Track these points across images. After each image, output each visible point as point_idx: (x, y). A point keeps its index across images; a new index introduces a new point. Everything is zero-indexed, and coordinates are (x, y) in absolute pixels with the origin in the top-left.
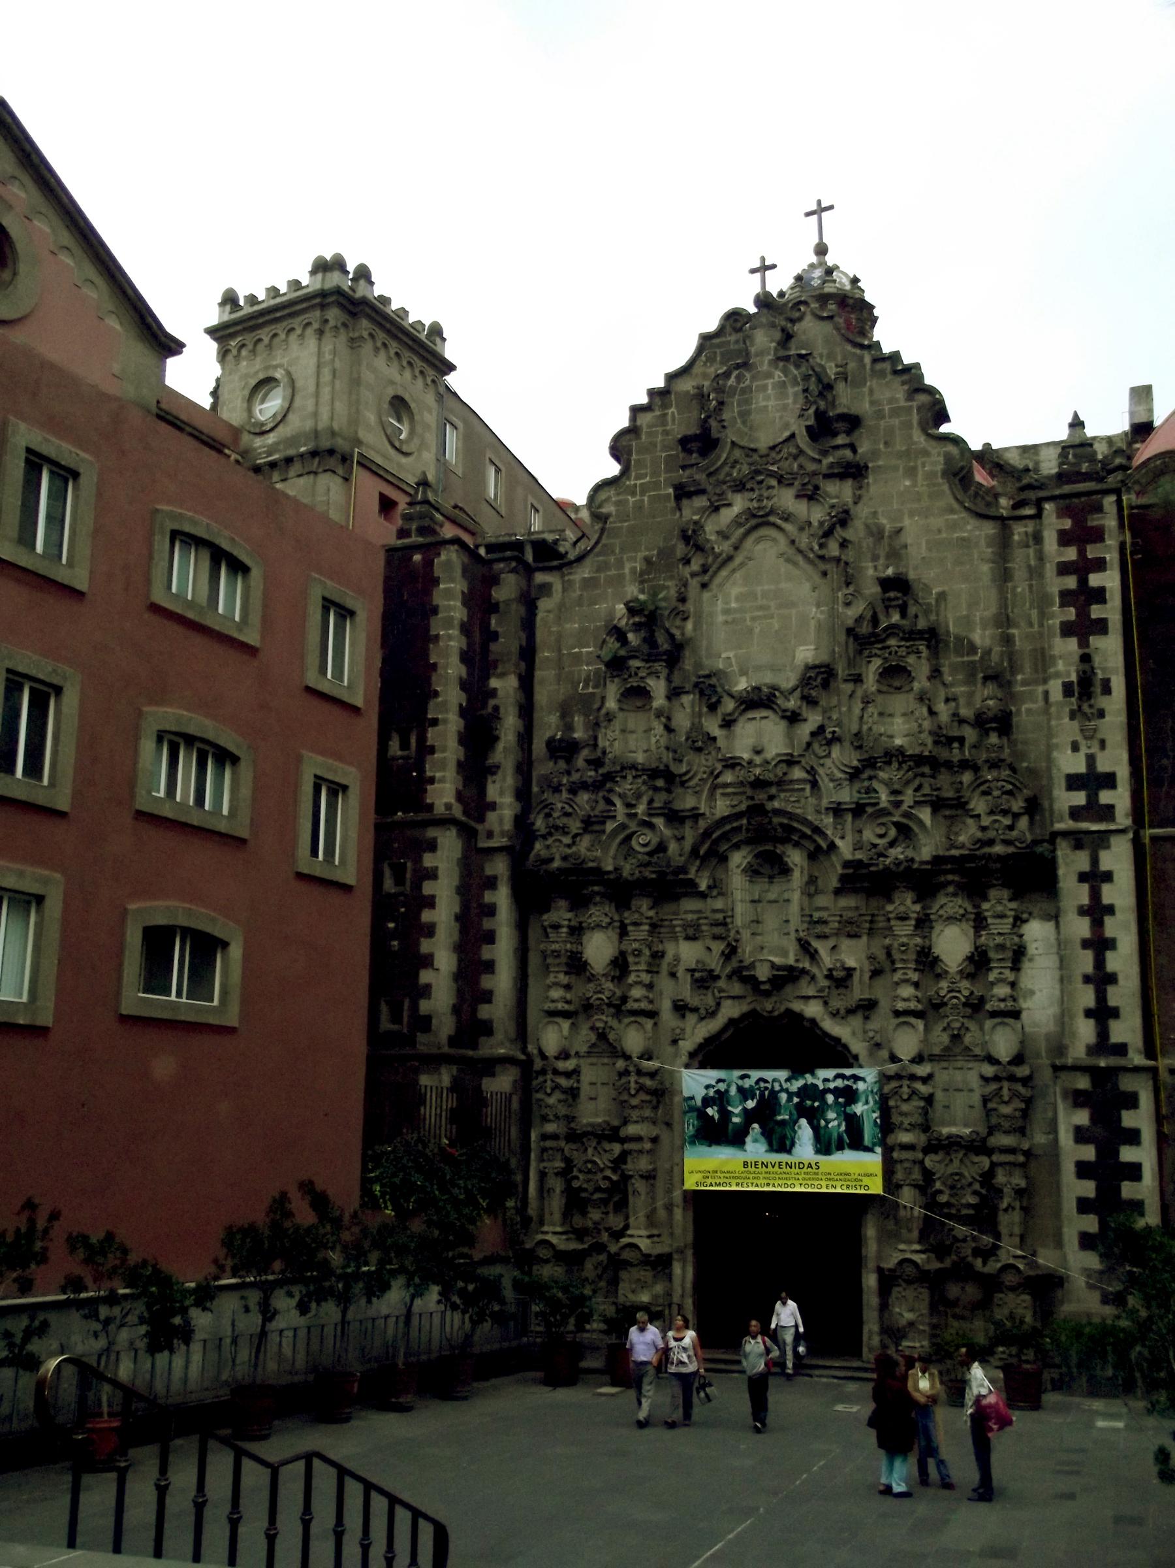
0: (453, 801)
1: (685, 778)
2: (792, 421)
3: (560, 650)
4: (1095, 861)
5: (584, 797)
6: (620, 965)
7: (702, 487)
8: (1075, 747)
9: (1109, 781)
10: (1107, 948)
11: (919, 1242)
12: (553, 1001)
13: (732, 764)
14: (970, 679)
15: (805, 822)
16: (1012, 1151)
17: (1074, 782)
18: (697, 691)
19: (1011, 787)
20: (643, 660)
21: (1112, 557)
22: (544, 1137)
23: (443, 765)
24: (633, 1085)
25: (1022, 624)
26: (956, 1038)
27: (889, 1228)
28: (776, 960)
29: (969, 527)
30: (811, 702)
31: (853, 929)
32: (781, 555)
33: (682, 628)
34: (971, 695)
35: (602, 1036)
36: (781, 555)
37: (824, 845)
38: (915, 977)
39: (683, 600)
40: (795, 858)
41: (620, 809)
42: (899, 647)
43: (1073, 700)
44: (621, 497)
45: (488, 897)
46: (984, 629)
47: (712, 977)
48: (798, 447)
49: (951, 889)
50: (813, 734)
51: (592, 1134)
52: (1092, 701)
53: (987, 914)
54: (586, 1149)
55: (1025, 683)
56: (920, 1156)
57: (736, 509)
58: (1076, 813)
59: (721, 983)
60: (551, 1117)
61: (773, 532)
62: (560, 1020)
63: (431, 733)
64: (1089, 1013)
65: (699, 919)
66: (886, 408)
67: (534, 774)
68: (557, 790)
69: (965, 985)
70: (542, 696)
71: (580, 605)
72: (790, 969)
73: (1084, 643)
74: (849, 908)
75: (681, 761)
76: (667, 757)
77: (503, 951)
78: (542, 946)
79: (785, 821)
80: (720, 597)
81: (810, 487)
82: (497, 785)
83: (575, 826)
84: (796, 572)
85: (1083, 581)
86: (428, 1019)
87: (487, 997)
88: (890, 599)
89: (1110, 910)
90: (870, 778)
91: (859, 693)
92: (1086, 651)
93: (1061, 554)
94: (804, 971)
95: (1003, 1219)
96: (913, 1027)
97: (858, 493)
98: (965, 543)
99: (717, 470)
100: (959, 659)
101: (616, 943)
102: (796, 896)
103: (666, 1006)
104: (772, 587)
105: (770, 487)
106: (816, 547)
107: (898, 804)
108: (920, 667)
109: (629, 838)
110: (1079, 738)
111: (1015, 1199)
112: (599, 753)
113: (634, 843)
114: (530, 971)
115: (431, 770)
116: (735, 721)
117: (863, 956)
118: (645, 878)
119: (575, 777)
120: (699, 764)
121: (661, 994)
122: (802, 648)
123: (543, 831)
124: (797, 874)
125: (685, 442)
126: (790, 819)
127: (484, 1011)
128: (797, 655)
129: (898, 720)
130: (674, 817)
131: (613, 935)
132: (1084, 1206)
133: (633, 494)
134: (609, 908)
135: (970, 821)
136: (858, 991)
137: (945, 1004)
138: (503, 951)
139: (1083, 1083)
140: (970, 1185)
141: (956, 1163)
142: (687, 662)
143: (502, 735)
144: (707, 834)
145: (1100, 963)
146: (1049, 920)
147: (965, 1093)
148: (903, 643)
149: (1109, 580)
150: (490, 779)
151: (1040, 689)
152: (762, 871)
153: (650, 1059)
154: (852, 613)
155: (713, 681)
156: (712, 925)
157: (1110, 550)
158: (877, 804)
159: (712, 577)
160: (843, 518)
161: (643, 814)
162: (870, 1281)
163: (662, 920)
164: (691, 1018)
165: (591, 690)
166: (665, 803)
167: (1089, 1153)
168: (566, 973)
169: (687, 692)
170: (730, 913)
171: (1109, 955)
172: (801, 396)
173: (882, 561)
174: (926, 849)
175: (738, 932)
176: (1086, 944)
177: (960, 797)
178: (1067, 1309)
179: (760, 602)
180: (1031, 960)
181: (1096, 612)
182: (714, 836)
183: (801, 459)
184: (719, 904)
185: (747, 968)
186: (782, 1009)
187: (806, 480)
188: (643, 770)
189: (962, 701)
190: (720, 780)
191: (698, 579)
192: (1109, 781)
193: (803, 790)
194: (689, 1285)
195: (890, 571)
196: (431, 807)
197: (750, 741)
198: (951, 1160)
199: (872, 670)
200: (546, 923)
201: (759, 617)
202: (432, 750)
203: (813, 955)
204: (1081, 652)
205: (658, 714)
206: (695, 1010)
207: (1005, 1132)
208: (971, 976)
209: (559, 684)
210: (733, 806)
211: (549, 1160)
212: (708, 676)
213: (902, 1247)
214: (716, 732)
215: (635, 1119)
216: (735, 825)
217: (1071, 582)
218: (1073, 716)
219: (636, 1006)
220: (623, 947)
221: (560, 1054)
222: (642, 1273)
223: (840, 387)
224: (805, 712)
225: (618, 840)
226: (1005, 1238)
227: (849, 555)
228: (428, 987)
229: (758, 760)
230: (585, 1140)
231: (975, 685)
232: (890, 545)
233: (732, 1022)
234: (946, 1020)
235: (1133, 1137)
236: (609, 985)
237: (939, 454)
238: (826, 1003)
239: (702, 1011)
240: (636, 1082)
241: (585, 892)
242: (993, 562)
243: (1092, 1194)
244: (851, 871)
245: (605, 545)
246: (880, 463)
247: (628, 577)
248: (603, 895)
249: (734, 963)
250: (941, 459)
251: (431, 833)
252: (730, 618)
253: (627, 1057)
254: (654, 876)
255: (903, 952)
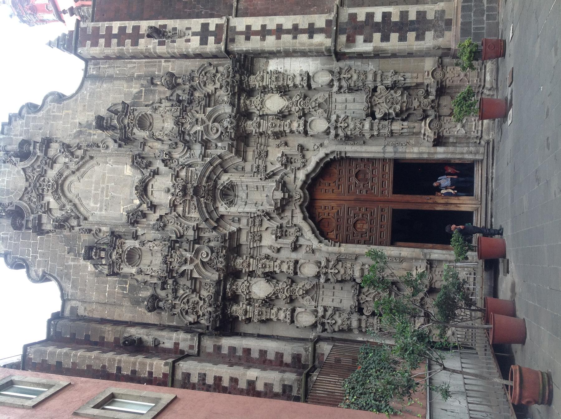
0: (164, 361)
1: (179, 235)
2: (17, 169)
3: (105, 303)
4: (241, 33)
5: (181, 292)
6: (270, 276)
7: (37, 217)
8: (188, 41)
9: (205, 26)
10: (281, 28)
11: (421, 123)
12: (286, 317)
13: (173, 206)
14: (153, 92)
15: (206, 168)
16: (375, 74)
17: (204, 41)
18: (136, 225)
19: (203, 73)
20: (113, 250)
21: (107, 24)
22: (360, 327)
23: (143, 364)
24: (332, 271)
25: (133, 71)
26: (320, 105)
27: (414, 143)
28: (273, 189)
29: (85, 93)
30: (149, 164)
31: (263, 154)
32: (79, 179)
33: (104, 232)
34: (160, 92)
35: (307, 292)
36: (79, 179)
37: (220, 160)
38: (289, 121)
39: (90, 231)
40: (225, 179)
41: (188, 267)
42: (129, 118)
43: (166, 41)
44: (36, 264)
45: (225, 351)
46: (132, 87)
47: (281, 227)
48: (29, 167)
49: (248, 102)
50: (166, 166)
51: (358, 296)
52: (167, 30)
53: (261, 85)
54: (367, 301)
55: (159, 71)
56: (376, 121)
57: (52, 200)
58: (218, 41)
59: (284, 222)
60: (349, 322)
61: (67, 183)
62: (295, 314)
63: (124, 372)
64: (311, 37)
65: (251, 233)
66: (25, 128)
67: (167, 324)
68: (174, 307)
69: (294, 99)
70: (127, 317)
71: (85, 290)
72: (278, 182)
73: (142, 36)
74: (253, 155)
75: (170, 237)
76: (166, 243)
77: (255, 345)
78: (256, 321)
79: (205, 179)
80: (93, 212)
81: (48, 161)
82: (165, 341)
83: (194, 298)
84: (88, 172)
85: (115, 36)
86: (284, 386)
87: (279, 356)
88: (107, 123)
89: (263, 27)
90: (189, 135)
91: (150, 144)
92: (145, 35)
93: (102, 45)
94: (282, 178)
95: (408, 81)
96: (312, 121)
97: (58, 141)
98: (92, 94)
99: (31, 209)
100: (143, 97)
101: (259, 279)
102: (243, 179)
103: (294, 256)
104: (93, 185)
105: (44, 181)
106: (77, 159)
107: (203, 122)
108: (142, 110)
109: (202, 262)
110: (184, 39)
111: (400, 74)
112: (160, 282)
113: (205, 260)
114: (270, 334)
115: (144, 374)
116: (151, 202)
117: (277, 149)
118: (224, 256)
119: (170, 297)
120: (172, 228)
121: (288, 258)
122: (125, 172)
123: (195, 317)
124: (233, 179)
125: (17, 227)
126: (204, 176)
127: (287, 359)
128: (128, 174)
129: (166, 125)
130: (198, 240)
131: (254, 280)
132: (402, 38)
133: (36, 257)
134: (240, 282)
135: (218, 93)
136: (292, 151)
137: (303, 109)
138: (255, 345)
139: (343, 38)
140: (392, 95)
141: (380, 101)
142: (121, 230)
143: (139, 336)
144: (206, 220)
145: (288, 32)
146: (269, 62)
147: (348, 104)
148: (128, 116)
149: (116, 26)
150: (161, 345)
151: (163, 64)
152: (231, 200)
153: (320, 263)
154: (112, 145)
155: (131, 214)
156: (254, 225)
157: (103, 25)
158: (202, 131)
159: (82, 214)
160: (67, 147)
161: (191, 254)
162: (441, 153)
163: (250, 254)
164: (301, 241)
165: (128, 286)
166: (187, 243)
167: (377, 36)
168: (272, 309)
169: (136, 231)
170: (249, 215)
171: (284, 27)
172: (7, 164)
173: (91, 132)
174: (226, 109)
175: (258, 210)
176: (278, 38)
177: (205, 96)
178: (453, 46)
179: (100, 192)
180: (286, 71)
181: (129, 31)
182: (208, 217)
183: (35, 167)
184: (244, 221)
185: (276, 204)
186: (300, 191)
187: (44, 162)
188: (168, 252)
189: (163, 96)
190: (181, 214)
191: (81, 221)
192: (205, 26)
193: (191, 171)
194: (444, 252)
195: (94, 124)
196: (165, 375)
197: (163, 194)
198: (379, 103)
199: (139, 134)
200: (244, 318)
201: (107, 193)
202: (134, 372)
203: (274, 174)
204: (146, 37)
205: (143, 244)
206: (297, 237)
207: (366, 79)
208: (291, 98)
209: (123, 306)
210: (195, 209)
211: (373, 326)
212: (128, 217)
213: (423, 131)
214: (157, 216)
215: (351, 272)
216: (203, 206)
217: (114, 41)
218: (174, 42)
219: (291, 268)
220: (259, 273)
221: (314, 314)
222: (437, 273)
223: (9, 148)
224: (154, 168)
225: (203, 270)
226: (419, 81)
227: (84, 145)
228: (266, 384)
229: (172, 190)
230: (362, 302)
231: (155, 90)
232: (85, 127)
233: (305, 219)
234: (311, 110)
235: (370, 16)
236: (281, 285)
237: (50, 105)
238: (299, 169)
239: (298, 234)
240: (331, 269)
241: (230, 295)
242: (103, 82)
243: (397, 35)
244: (234, 149)
245: (58, 275)
246: (48, 132)
247: (76, 263)
248: (232, 285)
249: (274, 215)
250: (52, 104)
251: (179, 376)
252: (104, 208)
253: (318, 276)
254: (224, 251)
255: (275, 125)
